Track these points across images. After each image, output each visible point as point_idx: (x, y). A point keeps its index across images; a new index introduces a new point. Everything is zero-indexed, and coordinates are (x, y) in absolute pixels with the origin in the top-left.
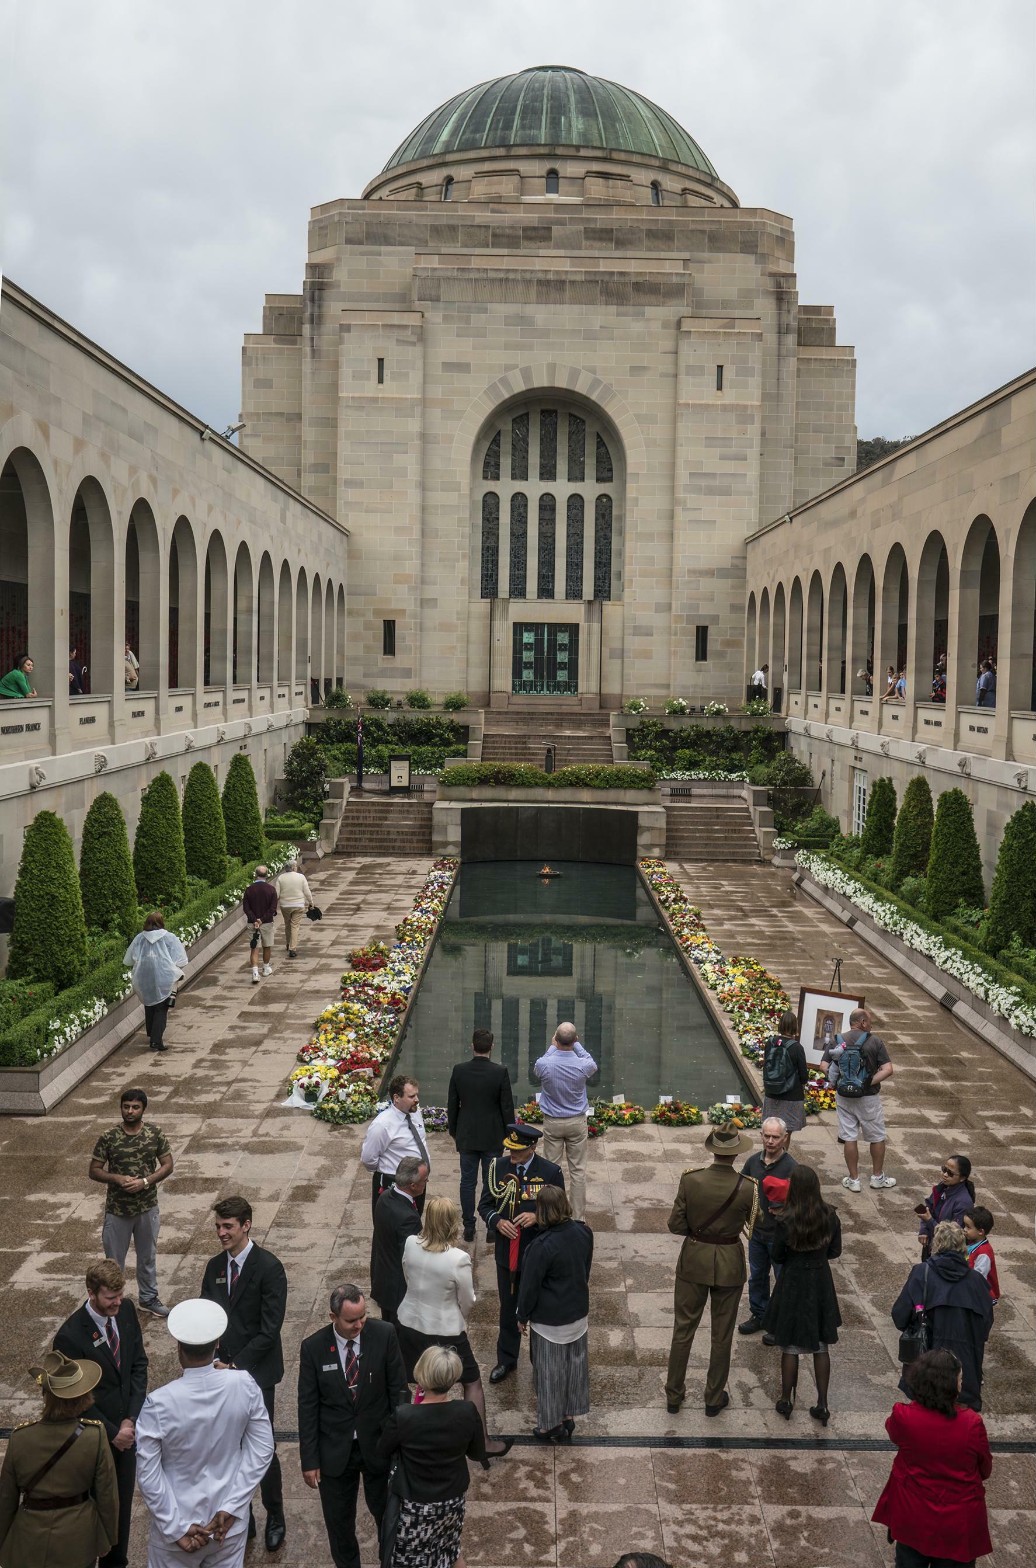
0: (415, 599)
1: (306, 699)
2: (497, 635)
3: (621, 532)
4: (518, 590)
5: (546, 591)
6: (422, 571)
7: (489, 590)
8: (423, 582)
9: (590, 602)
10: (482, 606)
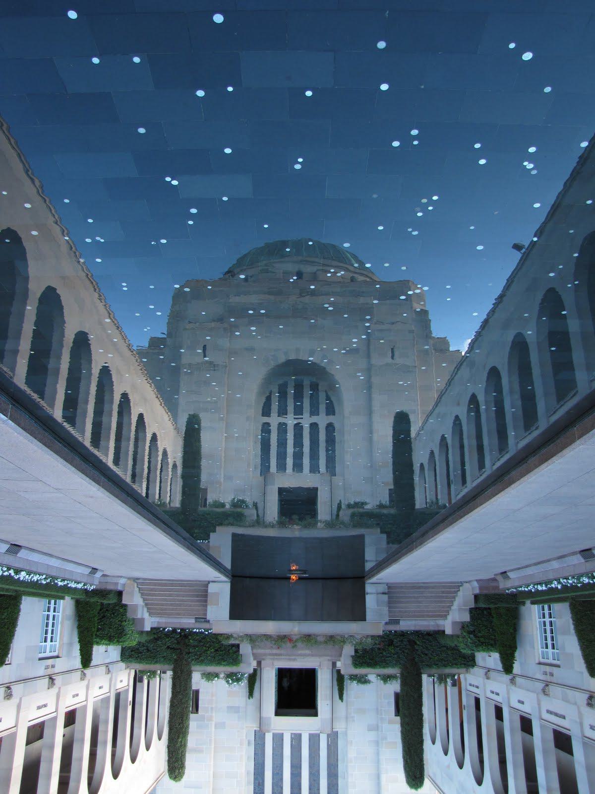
0: (382, 731)
1: (466, 679)
2: (329, 708)
3: (248, 773)
4: (314, 739)
5: (297, 739)
6: (378, 750)
7: (333, 737)
8: (377, 743)
9: (269, 732)
10: (339, 727)
